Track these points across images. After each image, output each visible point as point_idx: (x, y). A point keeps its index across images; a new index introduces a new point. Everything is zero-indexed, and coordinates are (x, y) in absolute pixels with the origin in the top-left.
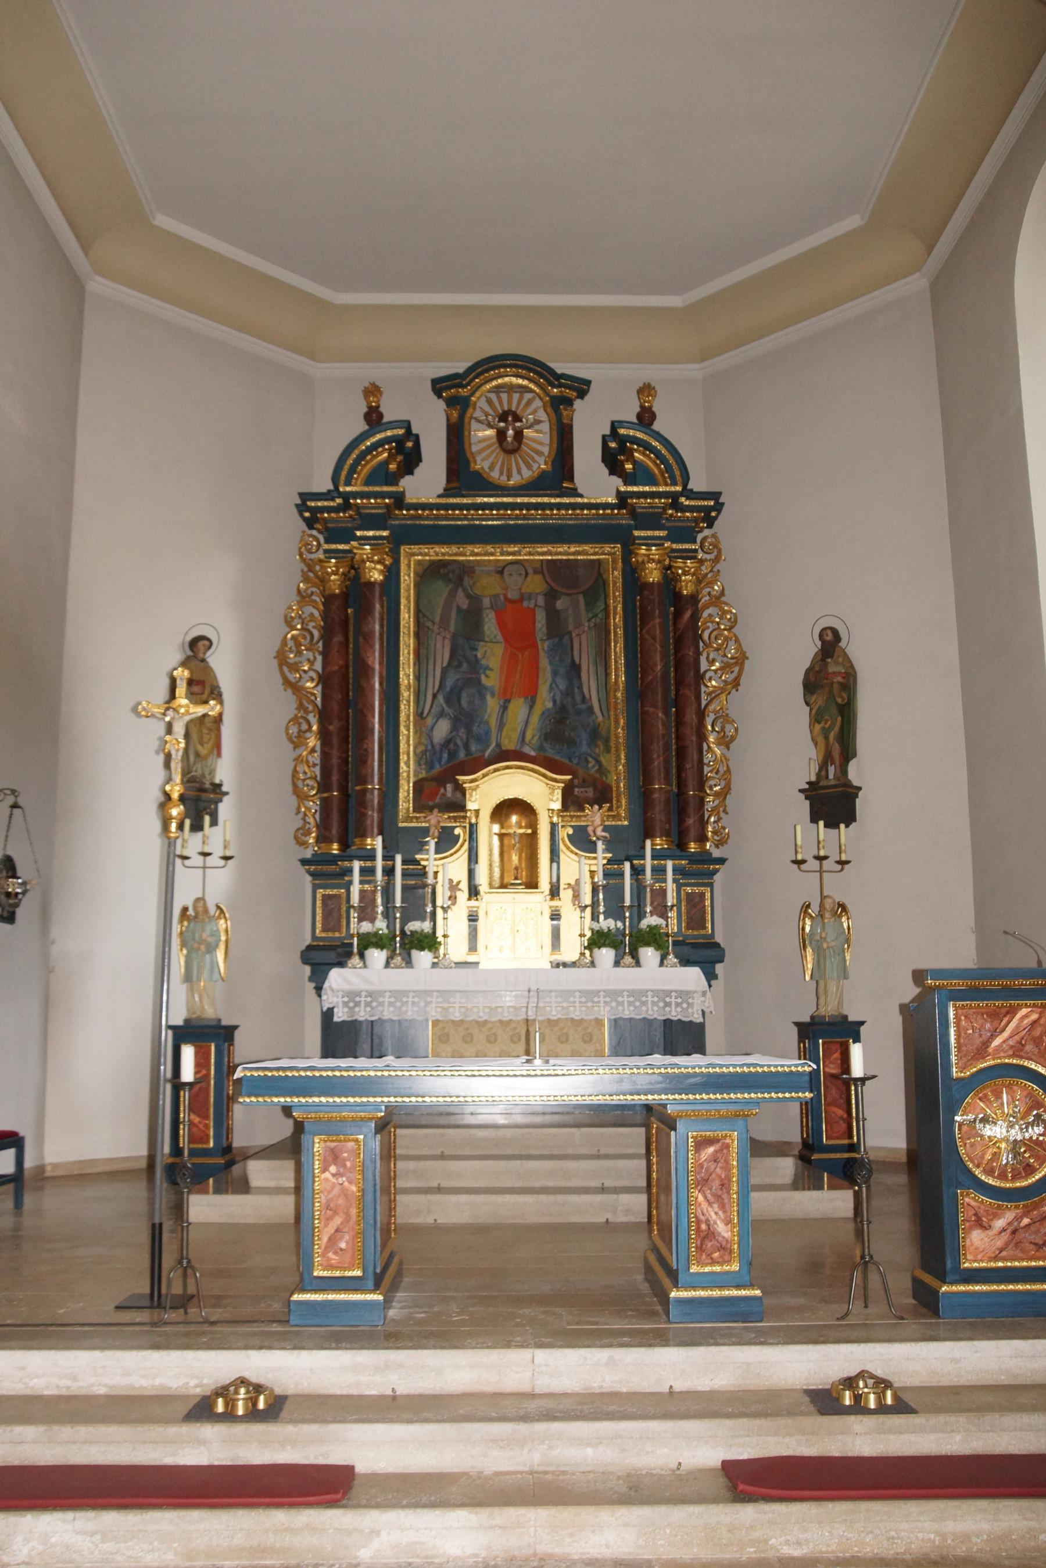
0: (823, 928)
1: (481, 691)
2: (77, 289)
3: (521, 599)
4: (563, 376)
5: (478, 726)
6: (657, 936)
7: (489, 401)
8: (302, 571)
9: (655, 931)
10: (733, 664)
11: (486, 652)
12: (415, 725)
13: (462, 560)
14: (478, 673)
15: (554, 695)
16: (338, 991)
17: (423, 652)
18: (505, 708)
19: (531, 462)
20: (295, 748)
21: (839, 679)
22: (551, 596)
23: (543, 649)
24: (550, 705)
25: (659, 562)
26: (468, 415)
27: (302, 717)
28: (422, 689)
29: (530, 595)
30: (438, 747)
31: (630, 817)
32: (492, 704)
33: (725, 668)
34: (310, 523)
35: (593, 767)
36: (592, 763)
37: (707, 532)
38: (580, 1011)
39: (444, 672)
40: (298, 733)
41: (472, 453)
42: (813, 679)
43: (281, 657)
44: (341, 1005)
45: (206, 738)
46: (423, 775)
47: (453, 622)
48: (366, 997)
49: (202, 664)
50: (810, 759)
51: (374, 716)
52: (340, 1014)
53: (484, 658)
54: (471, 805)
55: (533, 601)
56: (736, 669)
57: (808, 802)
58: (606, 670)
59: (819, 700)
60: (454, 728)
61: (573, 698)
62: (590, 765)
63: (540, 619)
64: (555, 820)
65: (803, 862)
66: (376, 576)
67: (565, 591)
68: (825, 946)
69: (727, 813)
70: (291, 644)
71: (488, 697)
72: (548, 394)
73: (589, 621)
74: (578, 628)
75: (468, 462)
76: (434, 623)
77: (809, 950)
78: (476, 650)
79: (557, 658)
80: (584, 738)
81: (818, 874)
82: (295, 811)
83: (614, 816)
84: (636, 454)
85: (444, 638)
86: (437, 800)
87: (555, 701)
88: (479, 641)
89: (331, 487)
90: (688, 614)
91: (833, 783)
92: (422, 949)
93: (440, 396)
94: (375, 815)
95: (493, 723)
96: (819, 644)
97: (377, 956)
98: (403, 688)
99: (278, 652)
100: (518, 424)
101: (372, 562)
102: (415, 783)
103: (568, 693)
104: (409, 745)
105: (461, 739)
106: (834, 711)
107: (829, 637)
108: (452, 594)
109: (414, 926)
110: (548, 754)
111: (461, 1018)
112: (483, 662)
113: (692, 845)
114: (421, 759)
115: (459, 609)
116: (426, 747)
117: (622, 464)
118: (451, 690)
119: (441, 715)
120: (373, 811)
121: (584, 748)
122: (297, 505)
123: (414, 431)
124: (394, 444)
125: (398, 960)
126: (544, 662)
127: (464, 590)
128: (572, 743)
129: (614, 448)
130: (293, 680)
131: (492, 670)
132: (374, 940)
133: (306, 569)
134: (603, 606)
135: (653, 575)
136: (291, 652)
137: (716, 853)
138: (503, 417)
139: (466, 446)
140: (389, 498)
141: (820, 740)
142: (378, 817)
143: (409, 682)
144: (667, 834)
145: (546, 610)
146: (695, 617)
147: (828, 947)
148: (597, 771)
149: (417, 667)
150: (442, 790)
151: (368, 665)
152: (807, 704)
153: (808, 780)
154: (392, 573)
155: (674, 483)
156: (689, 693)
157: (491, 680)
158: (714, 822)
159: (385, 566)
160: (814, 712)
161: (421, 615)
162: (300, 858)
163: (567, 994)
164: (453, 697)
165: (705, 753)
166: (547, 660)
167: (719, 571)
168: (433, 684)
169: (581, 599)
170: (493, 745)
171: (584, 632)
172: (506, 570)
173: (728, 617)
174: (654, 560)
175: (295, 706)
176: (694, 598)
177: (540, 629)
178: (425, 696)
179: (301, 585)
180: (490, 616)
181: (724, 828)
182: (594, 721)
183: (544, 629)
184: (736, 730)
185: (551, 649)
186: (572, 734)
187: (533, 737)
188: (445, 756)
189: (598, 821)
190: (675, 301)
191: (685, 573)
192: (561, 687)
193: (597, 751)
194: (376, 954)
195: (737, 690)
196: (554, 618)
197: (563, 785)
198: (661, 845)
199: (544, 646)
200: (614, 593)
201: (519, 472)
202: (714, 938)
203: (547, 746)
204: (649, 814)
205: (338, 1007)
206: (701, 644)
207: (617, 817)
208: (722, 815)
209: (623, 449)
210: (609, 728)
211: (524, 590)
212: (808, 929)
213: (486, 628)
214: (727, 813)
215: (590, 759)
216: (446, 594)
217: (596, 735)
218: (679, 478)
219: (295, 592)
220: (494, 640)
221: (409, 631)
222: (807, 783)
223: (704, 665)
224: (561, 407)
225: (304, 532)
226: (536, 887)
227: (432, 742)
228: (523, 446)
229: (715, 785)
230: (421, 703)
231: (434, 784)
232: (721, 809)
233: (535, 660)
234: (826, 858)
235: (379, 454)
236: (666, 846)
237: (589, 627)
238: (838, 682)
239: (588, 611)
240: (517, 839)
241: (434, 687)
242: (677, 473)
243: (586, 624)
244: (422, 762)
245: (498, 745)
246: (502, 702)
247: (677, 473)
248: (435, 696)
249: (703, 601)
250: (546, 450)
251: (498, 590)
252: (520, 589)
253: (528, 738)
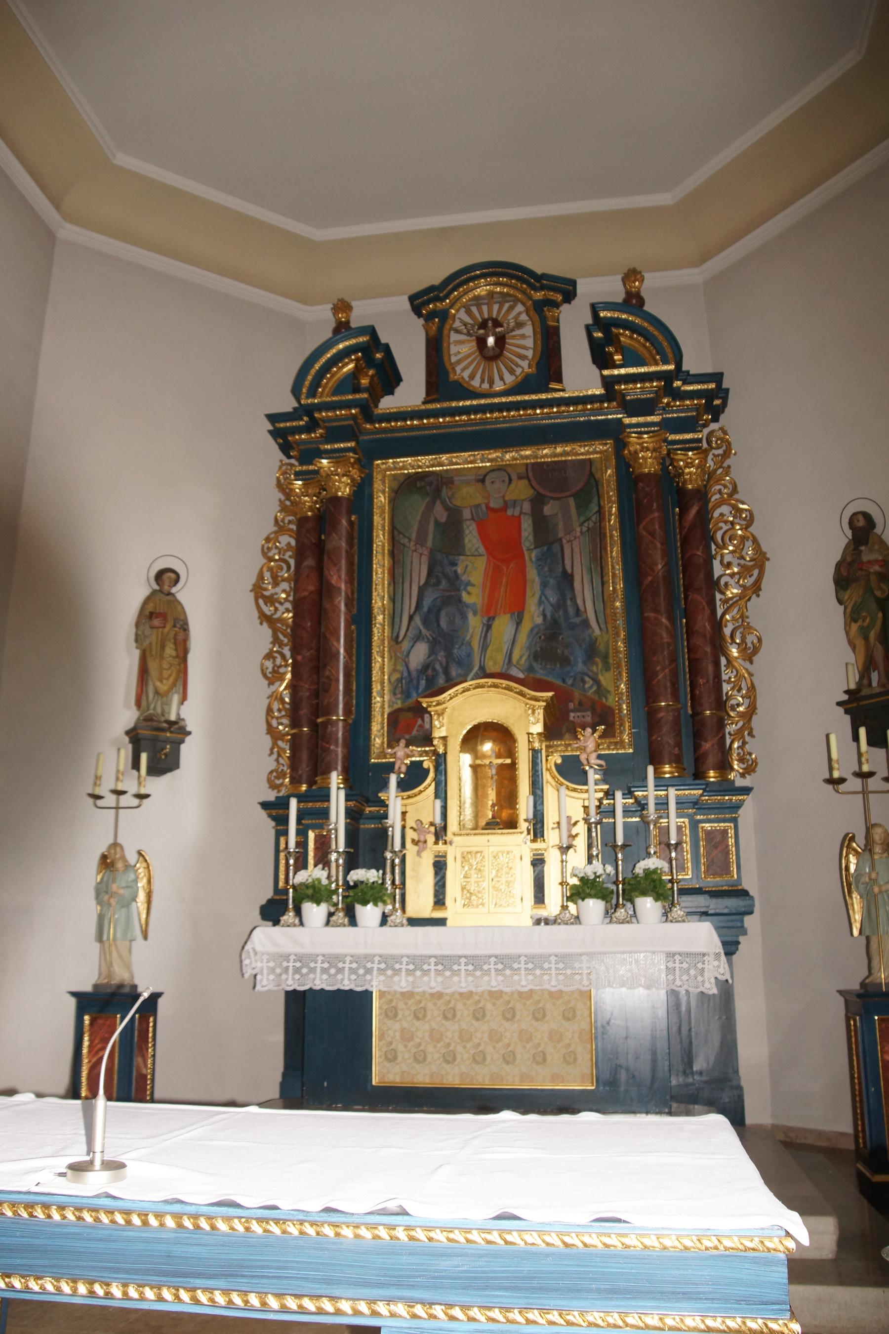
0: (873, 867)
1: (461, 609)
2: (49, 237)
3: (505, 508)
4: (544, 276)
5: (459, 648)
6: (658, 883)
7: (469, 312)
8: (280, 500)
9: (655, 877)
10: (752, 566)
11: (467, 567)
12: (389, 651)
13: (440, 471)
14: (459, 590)
15: (544, 610)
16: (263, 954)
17: (398, 571)
18: (488, 627)
19: (514, 367)
20: (269, 685)
21: (877, 568)
22: (538, 501)
23: (531, 559)
24: (539, 620)
25: (654, 450)
26: (447, 327)
27: (277, 652)
28: (398, 611)
29: (515, 501)
30: (414, 674)
31: (635, 743)
32: (475, 623)
33: (745, 571)
34: (285, 448)
35: (591, 687)
36: (589, 682)
37: (714, 426)
38: (557, 980)
39: (421, 591)
40: (273, 668)
41: (451, 364)
42: (845, 574)
43: (258, 589)
44: (265, 971)
45: (165, 674)
46: (399, 705)
47: (430, 536)
48: (295, 961)
49: (168, 598)
50: (847, 664)
51: (338, 641)
52: (265, 982)
53: (464, 573)
54: (437, 733)
55: (518, 509)
56: (756, 572)
57: (848, 717)
58: (602, 577)
59: (854, 594)
60: (432, 652)
61: (566, 611)
62: (587, 686)
63: (527, 527)
64: (537, 745)
65: (842, 780)
66: (344, 490)
67: (553, 495)
68: (876, 890)
69: (753, 736)
70: (267, 575)
71: (470, 615)
72: (530, 297)
73: (581, 525)
74: (569, 534)
75: (447, 373)
76: (410, 540)
77: (855, 895)
78: (456, 565)
79: (546, 569)
80: (579, 656)
81: (861, 795)
82: (269, 752)
83: (616, 744)
84: (622, 339)
85: (421, 554)
86: (414, 733)
87: (545, 616)
88: (459, 555)
89: (296, 405)
90: (694, 511)
91: (878, 690)
92: (365, 903)
93: (419, 314)
94: (340, 750)
95: (476, 645)
96: (849, 533)
97: (315, 912)
98: (376, 611)
99: (254, 585)
100: (499, 330)
101: (337, 475)
102: (389, 715)
103: (561, 605)
104: (383, 673)
105: (441, 664)
106: (873, 606)
107: (861, 523)
108: (430, 508)
110: (538, 676)
111: (409, 989)
112: (464, 578)
113: (712, 773)
114: (395, 688)
115: (437, 522)
116: (402, 674)
117: (611, 355)
118: (429, 610)
119: (418, 637)
120: (337, 746)
121: (580, 667)
122: (270, 432)
123: (383, 339)
124: (360, 354)
125: (340, 916)
126: (532, 574)
127: (443, 503)
128: (565, 661)
129: (599, 338)
130: (269, 613)
131: (473, 585)
132: (310, 892)
133: (283, 498)
134: (596, 509)
135: (648, 463)
136: (269, 583)
137: (740, 782)
138: (483, 325)
139: (446, 358)
140: (355, 407)
141: (860, 643)
142: (342, 752)
143: (383, 605)
144: (677, 760)
145: (532, 516)
146: (704, 516)
147: (881, 892)
148: (595, 692)
149: (392, 588)
150: (420, 722)
151: (332, 585)
152: (840, 602)
153: (846, 688)
155: (666, 362)
156: (699, 599)
157: (473, 597)
158: (738, 748)
159: (353, 480)
160: (849, 610)
161: (396, 532)
162: (261, 800)
164: (431, 618)
165: (723, 668)
166: (535, 571)
167: (729, 467)
168: (409, 604)
169: (572, 502)
170: (476, 668)
171: (575, 538)
172: (487, 478)
173: (744, 516)
174: (648, 449)
175: (271, 639)
176: (702, 495)
177: (527, 538)
178: (401, 618)
179: (279, 514)
180: (471, 528)
181: (750, 754)
182: (590, 636)
183: (531, 538)
184: (760, 640)
185: (539, 559)
186: (566, 652)
187: (521, 657)
188: (423, 683)
189: (591, 745)
190: (665, 199)
191: (688, 465)
192: (551, 599)
193: (595, 668)
194: (315, 910)
195: (758, 596)
196: (542, 526)
197: (544, 704)
198: (670, 773)
199: (531, 556)
200: (608, 493)
201: (502, 379)
202: (741, 885)
203: (536, 666)
204: (654, 738)
205: (262, 974)
206: (713, 547)
207: (621, 744)
208: (747, 738)
209: (611, 339)
210: (607, 643)
211: (506, 498)
212: (852, 868)
213: (466, 540)
214: (753, 736)
215: (587, 679)
216: (423, 507)
217: (592, 652)
218: (670, 356)
219: (272, 522)
220: (476, 553)
221: (383, 549)
222: (846, 692)
223: (718, 570)
224: (545, 309)
225: (281, 461)
226: (516, 828)
227: (408, 668)
228: (505, 352)
229: (738, 705)
230: (397, 627)
231: (410, 715)
232: (746, 730)
233: (522, 571)
234: (871, 774)
235: (347, 364)
236: (676, 774)
237: (581, 533)
238: (876, 573)
239: (579, 514)
240: (494, 771)
241: (410, 609)
242: (668, 350)
243: (578, 529)
244: (397, 691)
245: (482, 668)
246: (485, 620)
247: (668, 350)
248: (411, 618)
249: (713, 499)
250: (530, 354)
251: (479, 500)
252: (504, 497)
253: (515, 657)
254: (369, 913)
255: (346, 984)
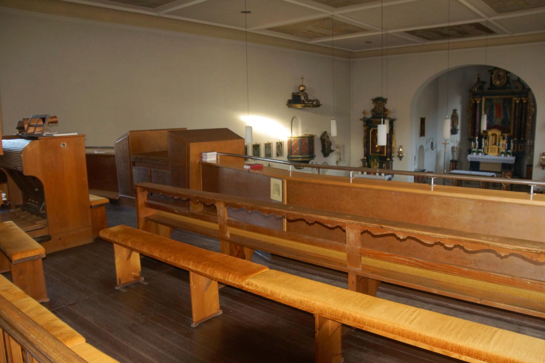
32: (494, 118)
63: (502, 107)
109: (480, 150)
154: (481, 102)
157: (494, 115)
163: (496, 160)
254: (480, 154)
255: (478, 160)
